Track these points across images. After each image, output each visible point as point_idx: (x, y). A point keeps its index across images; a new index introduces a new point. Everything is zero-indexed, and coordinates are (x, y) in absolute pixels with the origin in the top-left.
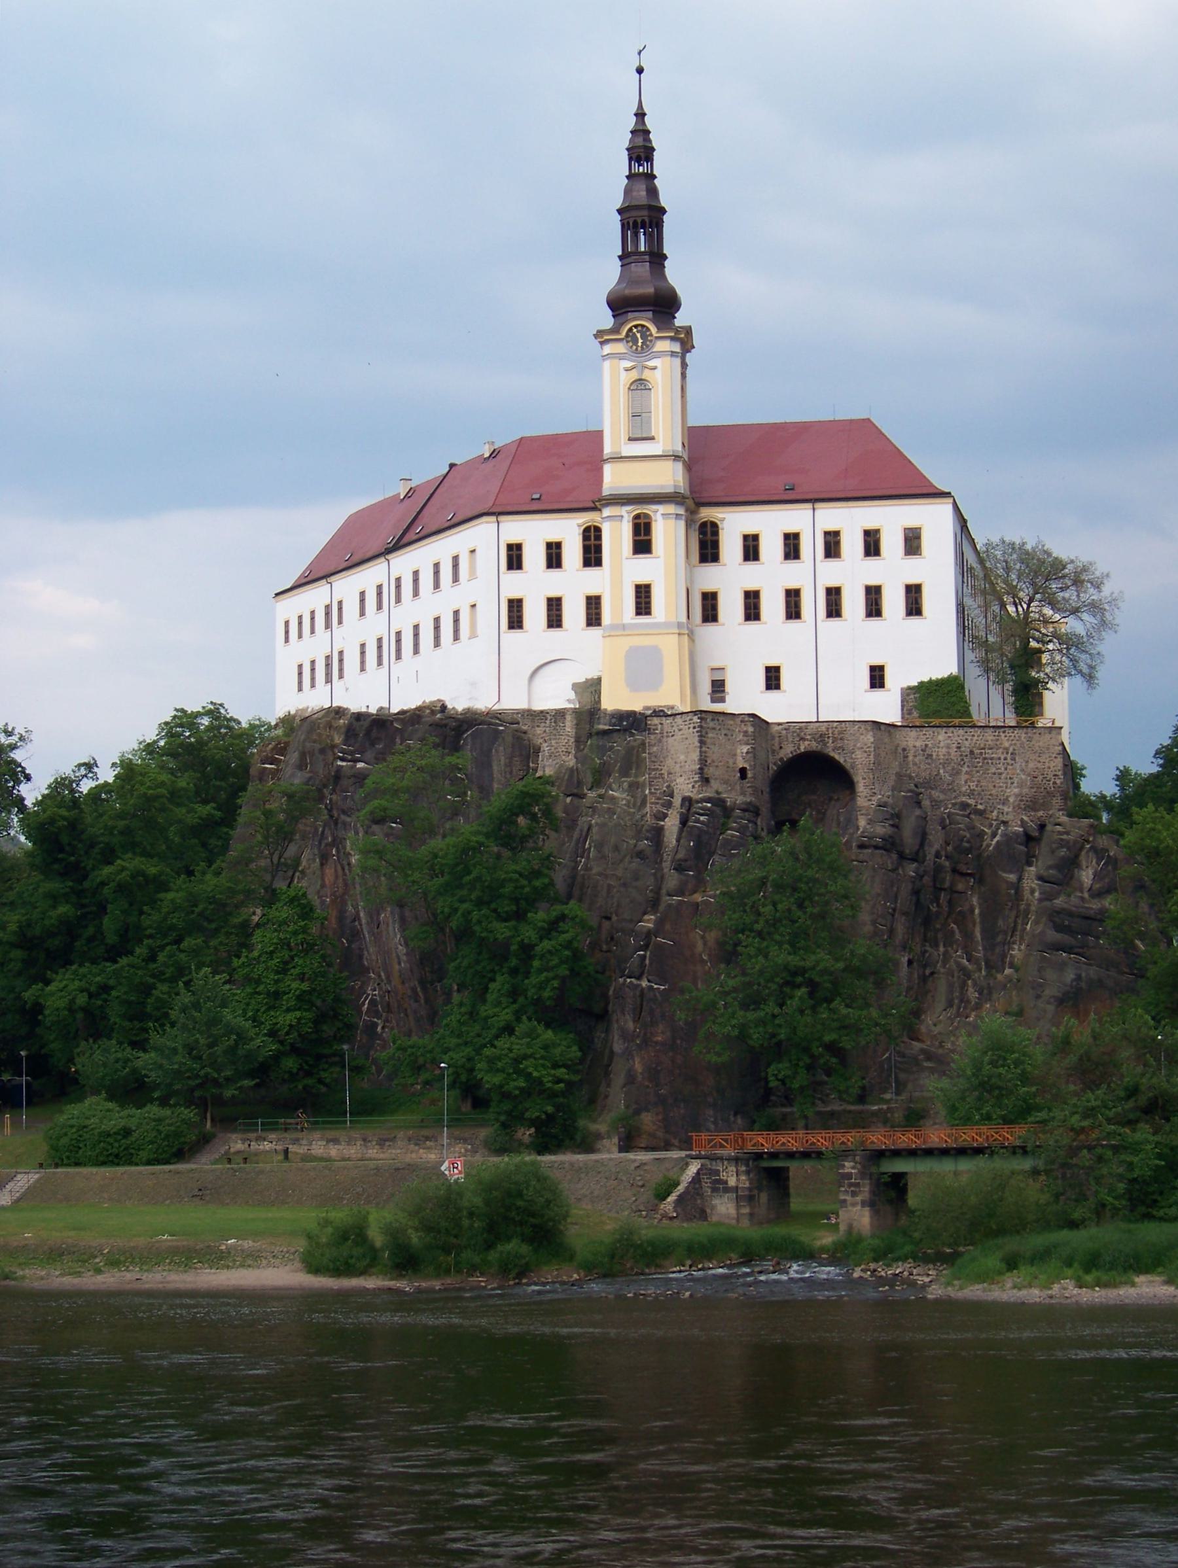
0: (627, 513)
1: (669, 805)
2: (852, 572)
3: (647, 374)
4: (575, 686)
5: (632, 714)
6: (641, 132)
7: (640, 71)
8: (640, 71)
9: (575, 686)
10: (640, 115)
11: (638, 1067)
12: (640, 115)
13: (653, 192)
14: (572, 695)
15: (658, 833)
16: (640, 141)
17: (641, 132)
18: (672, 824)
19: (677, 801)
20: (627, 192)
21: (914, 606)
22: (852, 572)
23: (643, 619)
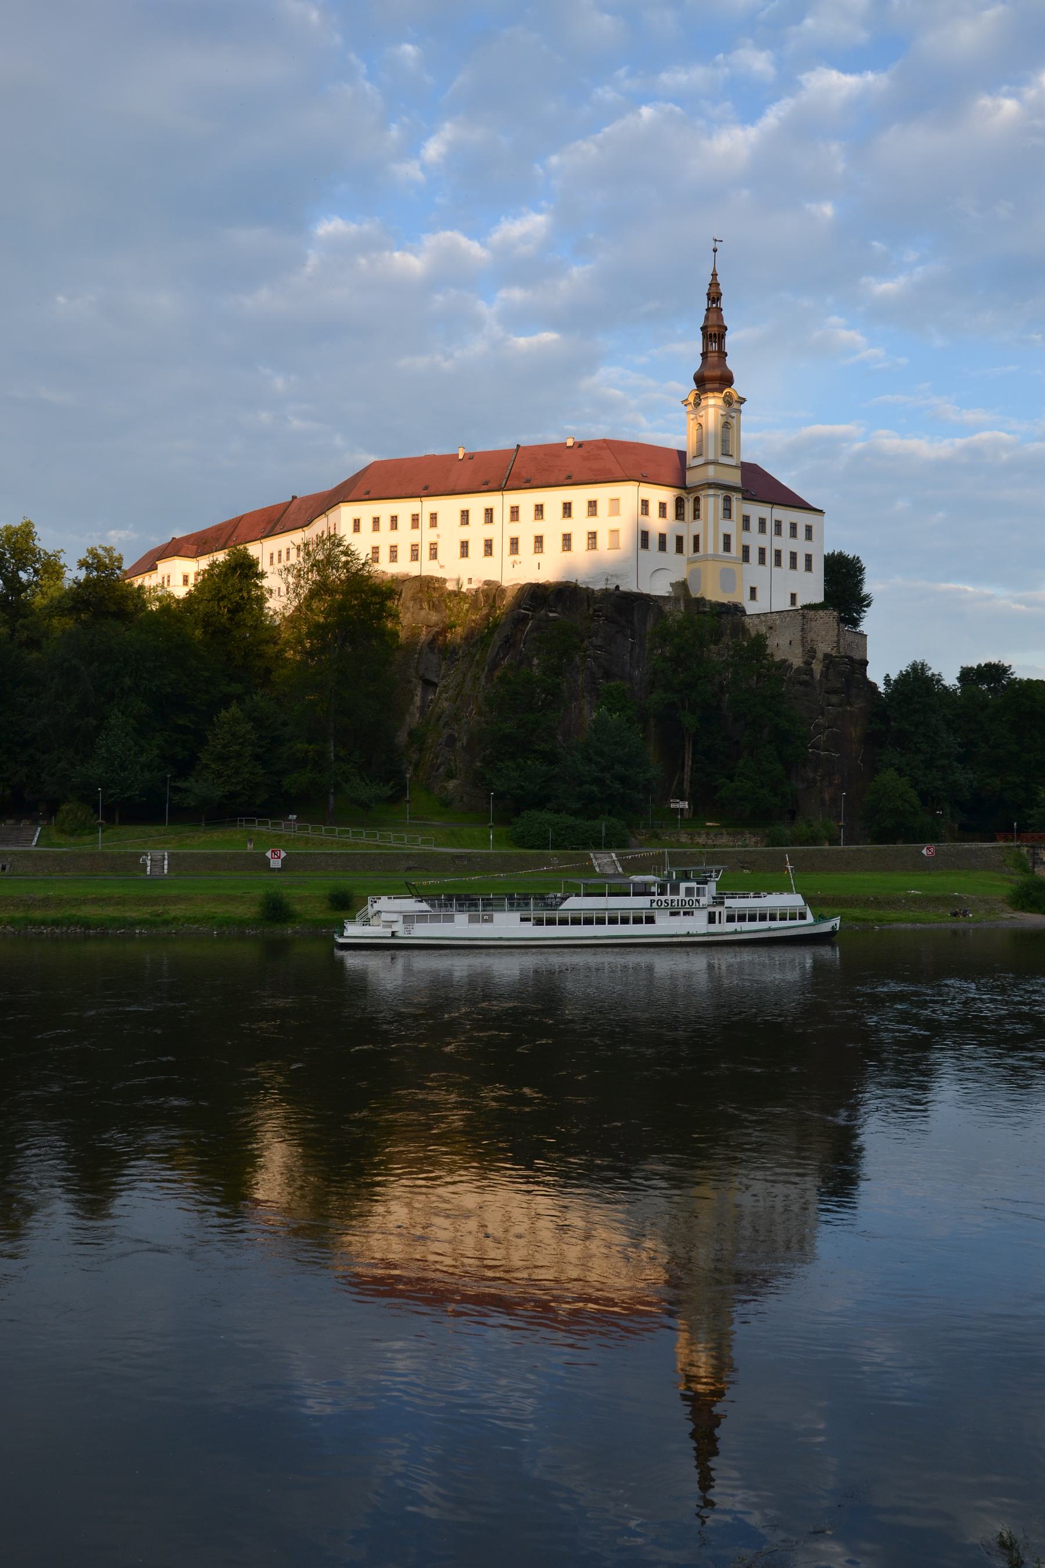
0: (722, 493)
1: (813, 657)
2: (785, 544)
3: (730, 420)
4: (672, 585)
5: (723, 604)
6: (714, 284)
7: (715, 251)
8: (715, 251)
9: (672, 585)
10: (714, 275)
11: (827, 797)
12: (714, 275)
13: (720, 318)
14: (671, 589)
15: (810, 672)
16: (714, 289)
17: (714, 284)
18: (817, 667)
19: (820, 655)
20: (707, 318)
21: (809, 567)
22: (785, 544)
23: (726, 554)
